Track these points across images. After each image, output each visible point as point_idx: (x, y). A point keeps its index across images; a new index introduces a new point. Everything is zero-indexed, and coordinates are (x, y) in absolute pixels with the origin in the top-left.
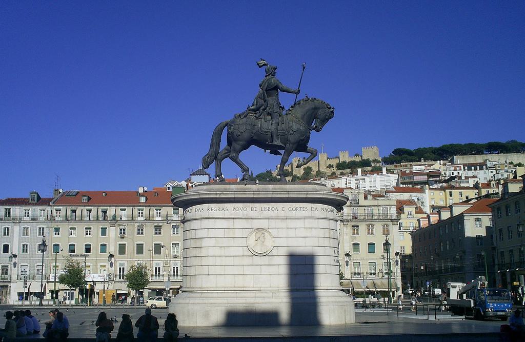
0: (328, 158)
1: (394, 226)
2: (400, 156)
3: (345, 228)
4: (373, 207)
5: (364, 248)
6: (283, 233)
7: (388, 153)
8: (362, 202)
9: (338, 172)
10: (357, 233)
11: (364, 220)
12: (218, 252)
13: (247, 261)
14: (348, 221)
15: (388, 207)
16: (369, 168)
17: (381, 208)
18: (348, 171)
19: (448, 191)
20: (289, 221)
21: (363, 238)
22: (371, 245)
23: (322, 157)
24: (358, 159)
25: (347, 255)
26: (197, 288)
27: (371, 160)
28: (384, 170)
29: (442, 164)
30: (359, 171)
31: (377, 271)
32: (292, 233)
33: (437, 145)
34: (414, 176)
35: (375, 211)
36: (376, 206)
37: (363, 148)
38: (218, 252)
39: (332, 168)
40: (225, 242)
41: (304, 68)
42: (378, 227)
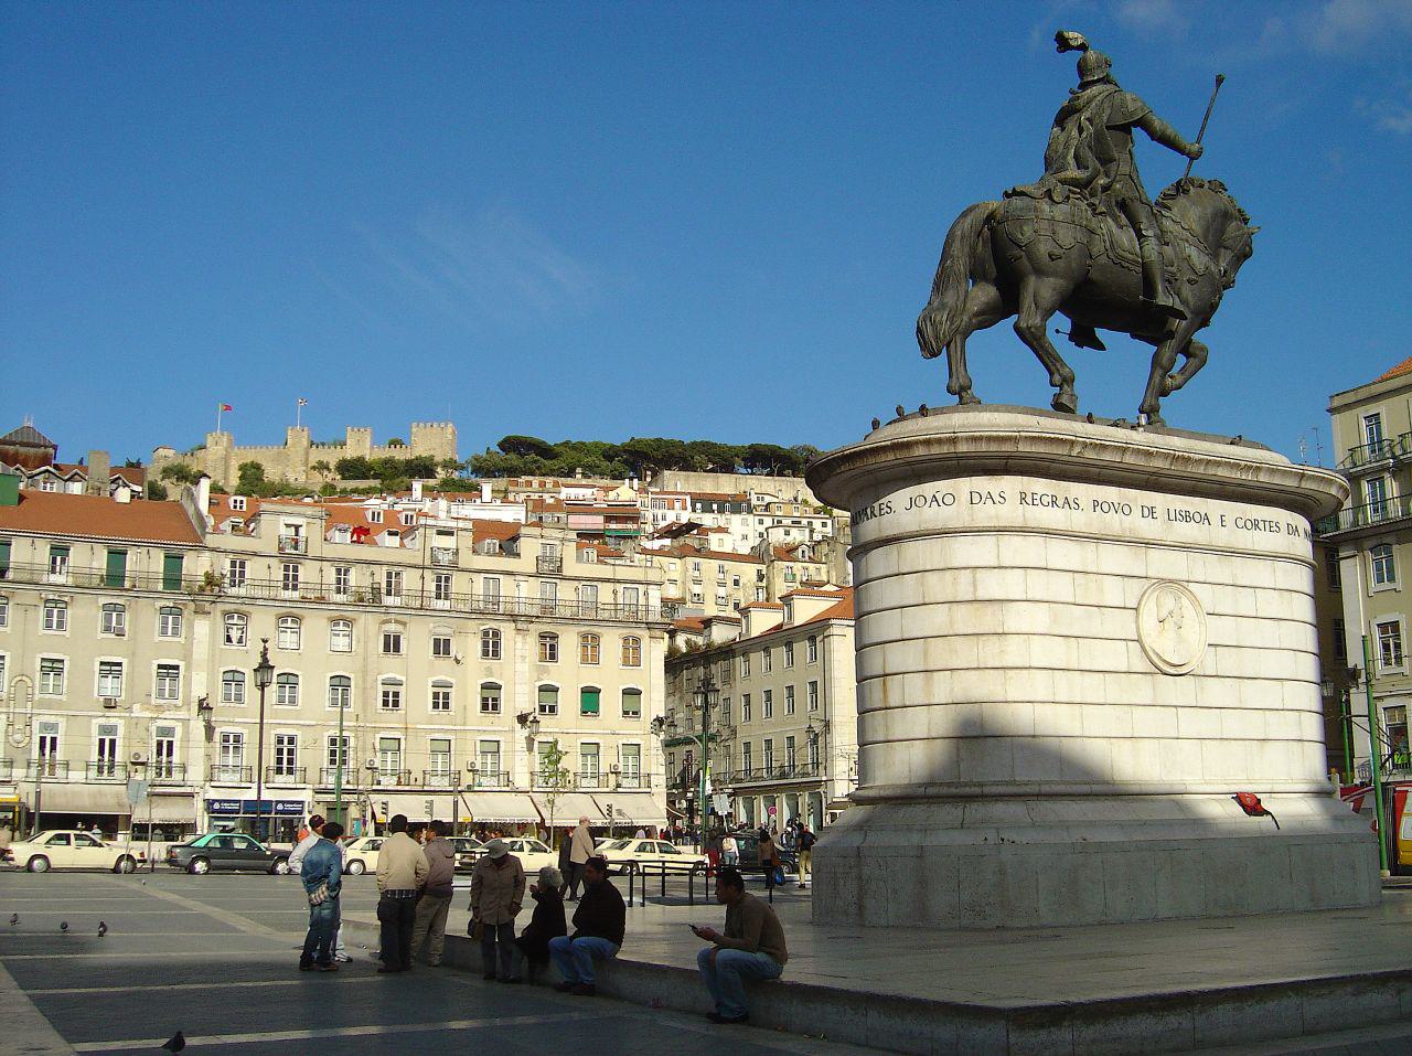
0: (312, 443)
2: (523, 457)
3: (519, 638)
4: (599, 585)
5: (569, 701)
6: (1224, 600)
7: (486, 443)
12: (1057, 652)
13: (1142, 689)
14: (530, 619)
15: (641, 588)
16: (431, 482)
18: (375, 483)
19: (690, 561)
20: (1237, 561)
21: (569, 674)
22: (590, 696)
23: (298, 438)
24: (400, 455)
25: (522, 719)
26: (996, 783)
27: (438, 458)
29: (636, 487)
31: (604, 768)
32: (1245, 602)
33: (618, 437)
34: (569, 513)
35: (605, 593)
36: (608, 580)
37: (414, 424)
38: (1057, 652)
39: (326, 473)
40: (1077, 621)
41: (1219, 80)
42: (611, 642)
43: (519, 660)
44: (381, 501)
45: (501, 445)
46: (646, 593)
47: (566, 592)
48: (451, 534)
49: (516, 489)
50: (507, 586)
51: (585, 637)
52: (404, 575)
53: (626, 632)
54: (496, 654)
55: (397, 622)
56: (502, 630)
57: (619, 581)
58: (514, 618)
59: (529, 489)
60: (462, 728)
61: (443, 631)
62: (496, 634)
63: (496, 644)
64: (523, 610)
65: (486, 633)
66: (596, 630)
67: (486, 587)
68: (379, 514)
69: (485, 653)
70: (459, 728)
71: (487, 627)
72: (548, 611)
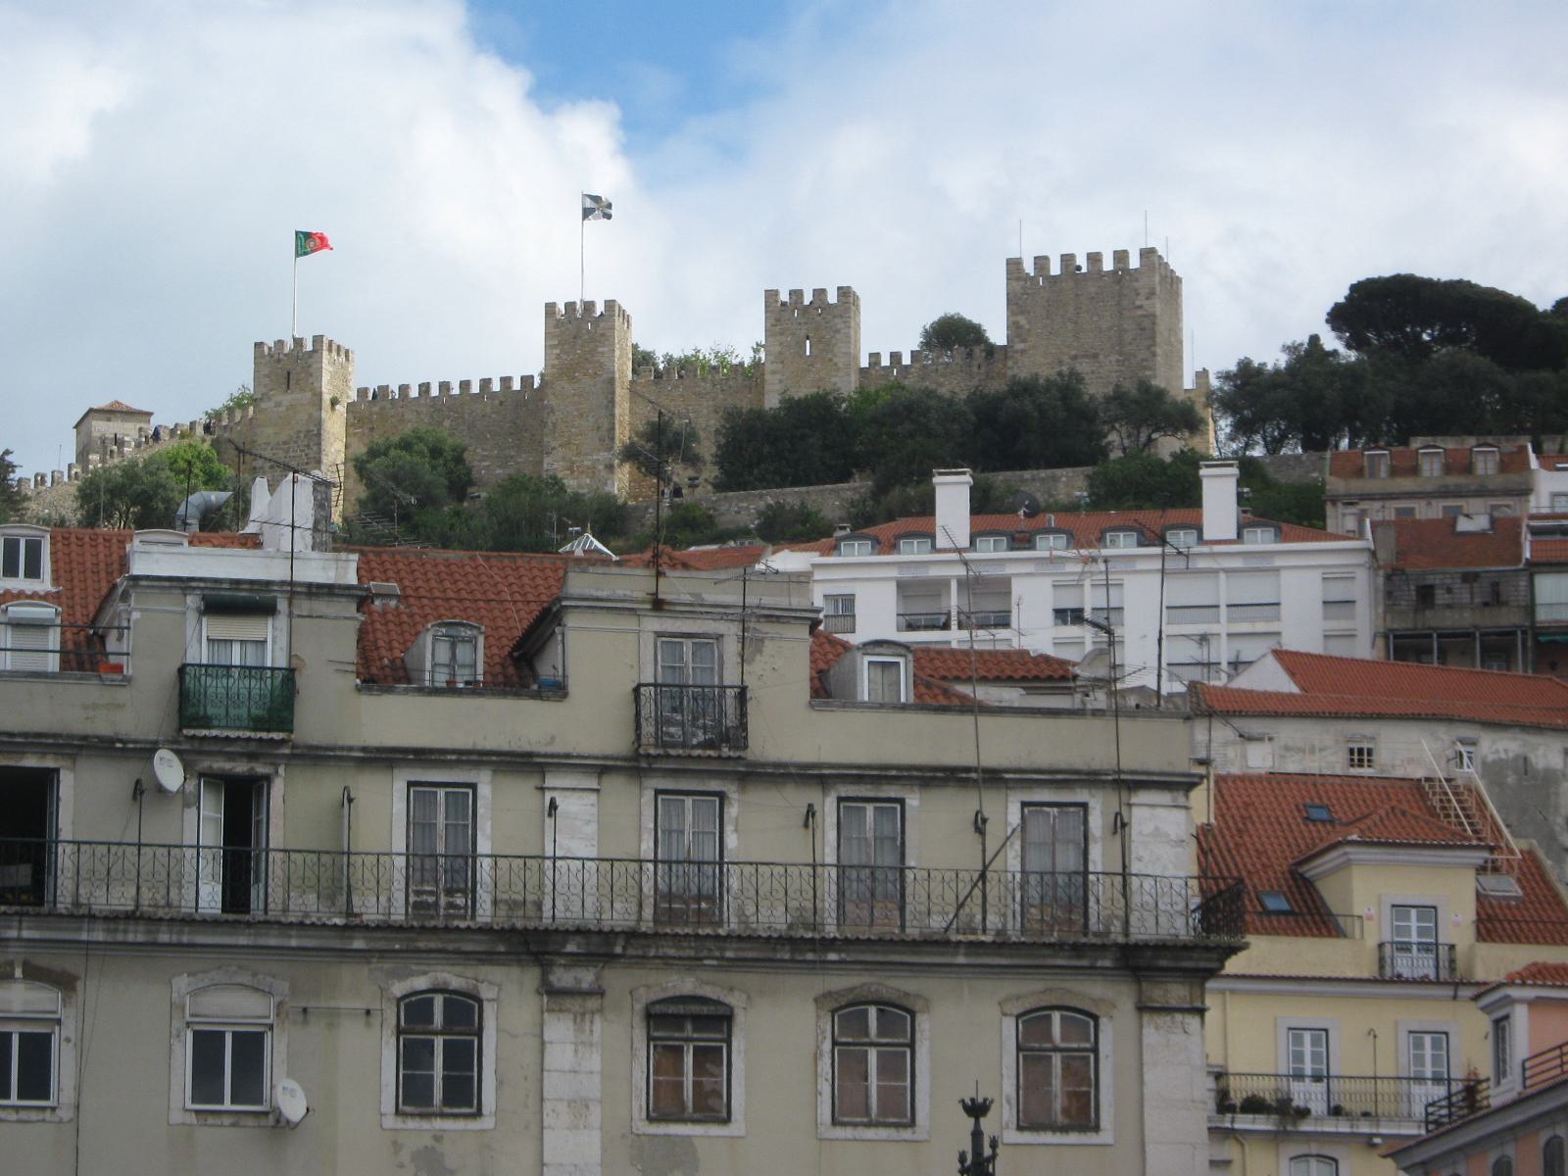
1: (1154, 1032)
3: (559, 1029)
8: (786, 726)
9: (745, 508)
10: (712, 1108)
11: (793, 950)
16: (1071, 484)
17: (1006, 810)
27: (1096, 386)
28: (1219, 494)
30: (953, 496)
39: (679, 472)
43: (557, 1118)
44: (815, 558)
45: (1338, 317)
46: (1120, 825)
48: (267, 610)
49: (1357, 485)
50: (500, 815)
51: (847, 1012)
52: (67, 785)
53: (1030, 990)
54: (462, 1093)
55: (35, 974)
56: (486, 992)
57: (994, 778)
58: (532, 945)
59: (1406, 484)
61: (235, 1006)
62: (464, 1011)
63: (463, 1060)
65: (415, 1009)
67: (419, 826)
68: (34, 548)
69: (413, 1094)
71: (421, 983)
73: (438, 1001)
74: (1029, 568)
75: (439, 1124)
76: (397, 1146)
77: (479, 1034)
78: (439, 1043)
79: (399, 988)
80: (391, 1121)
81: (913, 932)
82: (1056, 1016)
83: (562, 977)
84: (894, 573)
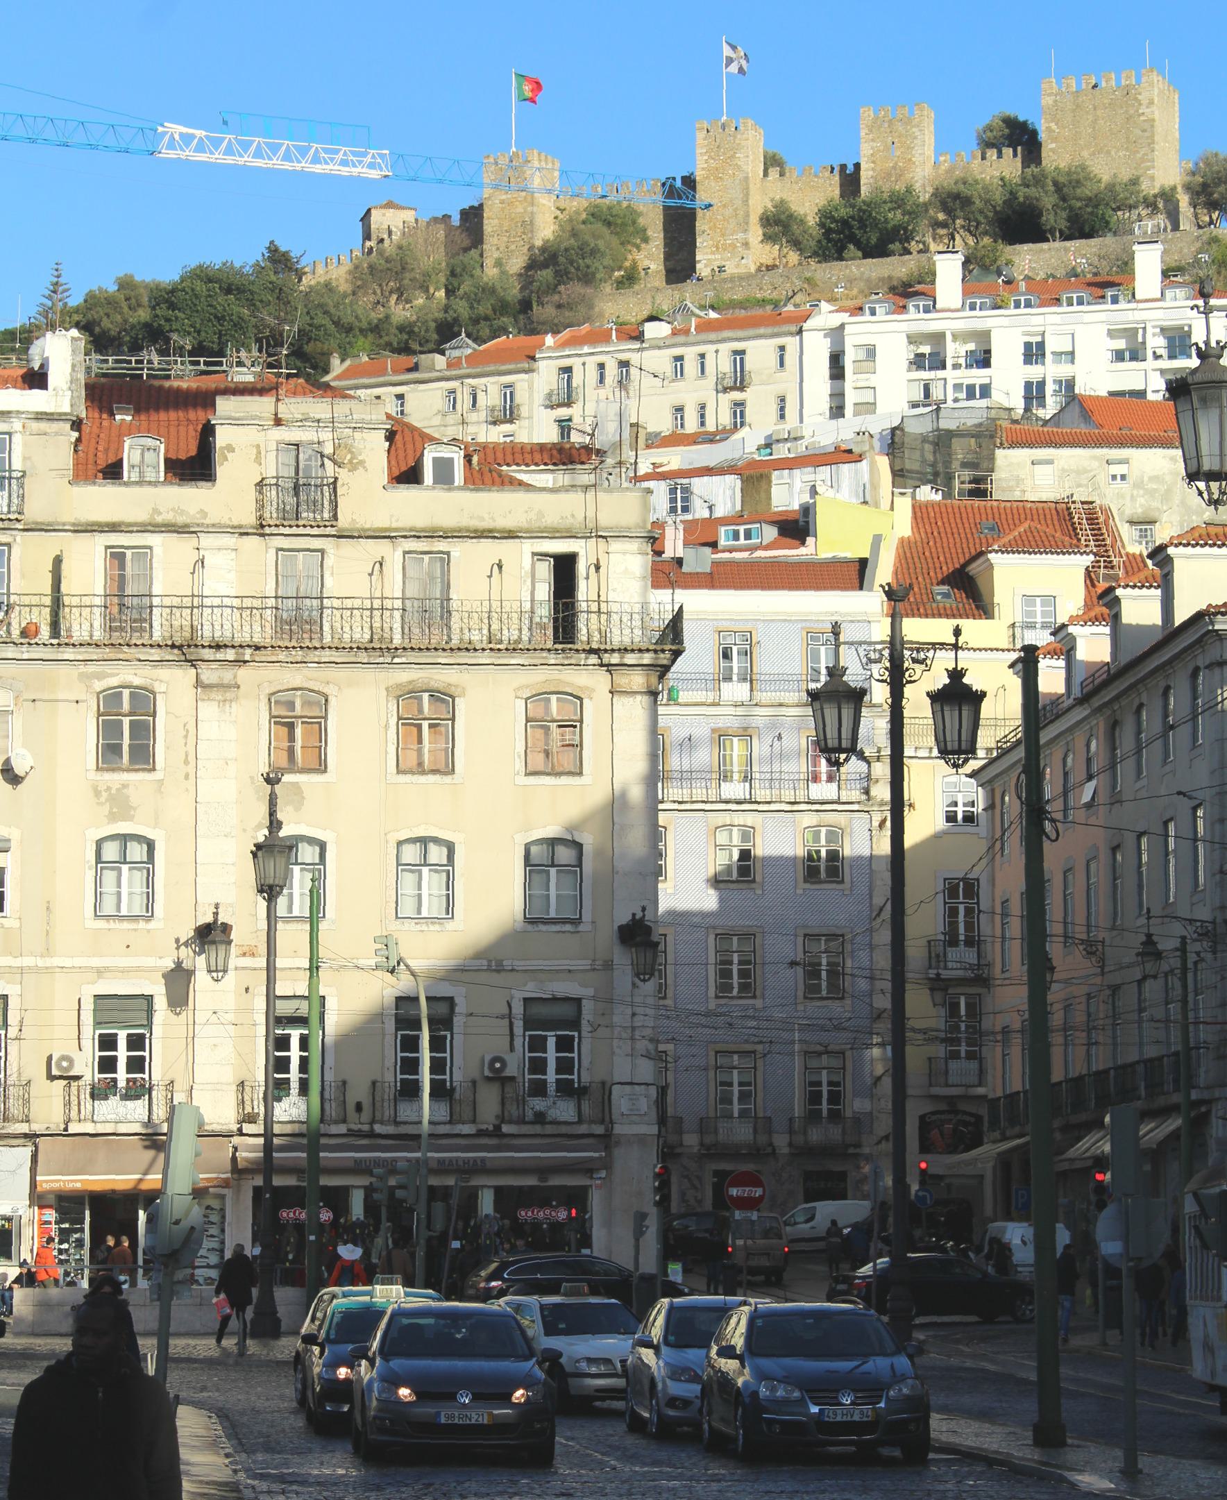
3: (209, 710)
47: (347, 574)
53: (538, 678)
54: (143, 756)
56: (158, 687)
60: (41, 963)
62: (144, 701)
63: (143, 732)
64: (215, 626)
65: (111, 698)
66: (442, 677)
70: (28, 961)
71: (114, 682)
72: (298, 626)
73: (126, 693)
74: (1005, 321)
75: (126, 777)
76: (97, 793)
77: (154, 715)
78: (126, 721)
79: (99, 685)
80: (93, 775)
81: (455, 642)
82: (554, 698)
83: (209, 674)
84: (904, 327)
